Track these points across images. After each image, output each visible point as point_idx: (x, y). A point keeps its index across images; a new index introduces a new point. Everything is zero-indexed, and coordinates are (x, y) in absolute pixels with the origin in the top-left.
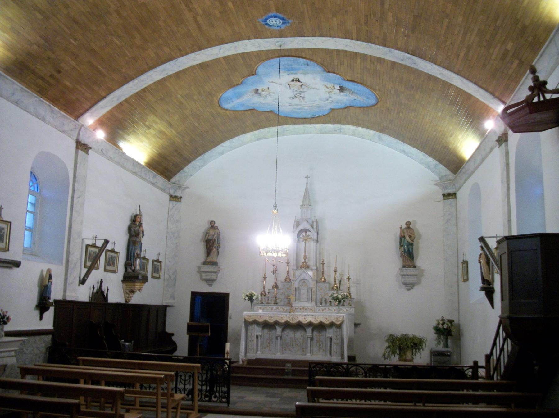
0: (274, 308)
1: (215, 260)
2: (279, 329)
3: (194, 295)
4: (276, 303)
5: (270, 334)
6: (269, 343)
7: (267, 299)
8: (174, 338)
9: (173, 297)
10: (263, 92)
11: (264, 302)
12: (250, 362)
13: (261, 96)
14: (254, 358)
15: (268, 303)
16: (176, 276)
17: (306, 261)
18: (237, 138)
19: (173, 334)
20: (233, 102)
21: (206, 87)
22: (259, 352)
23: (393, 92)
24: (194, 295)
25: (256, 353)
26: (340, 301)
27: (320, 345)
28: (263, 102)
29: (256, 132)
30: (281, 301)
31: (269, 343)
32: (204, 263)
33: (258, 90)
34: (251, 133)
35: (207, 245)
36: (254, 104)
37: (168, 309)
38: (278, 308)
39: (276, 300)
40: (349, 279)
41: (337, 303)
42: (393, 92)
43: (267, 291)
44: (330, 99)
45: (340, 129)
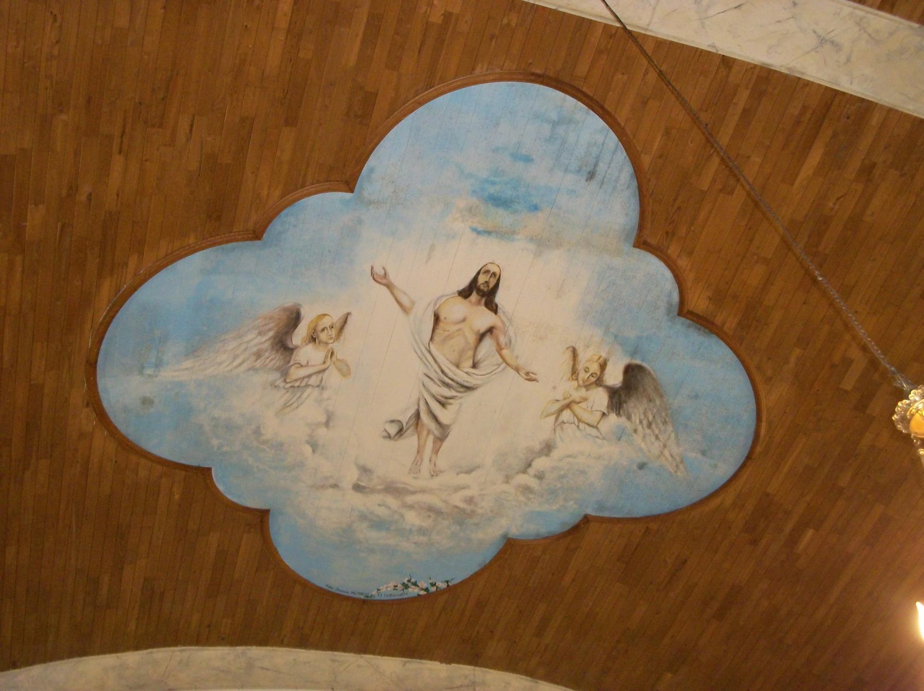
10: (310, 347)
13: (284, 373)
18: (37, 670)
20: (159, 365)
21: (118, 163)
23: (848, 384)
28: (272, 428)
29: (132, 658)
33: (294, 318)
34: (109, 660)
36: (230, 427)
42: (848, 384)
44: (541, 463)
45: (474, 684)
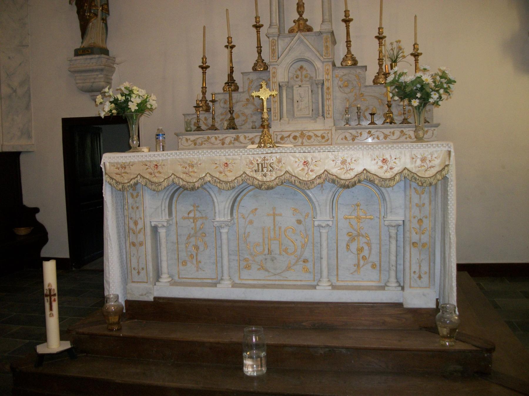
0: (227, 141)
1: (100, 44)
2: (222, 203)
3: (66, 122)
4: (232, 126)
5: (195, 219)
6: (197, 248)
7: (210, 121)
8: (39, 217)
9: (27, 133)
11: (203, 127)
12: (136, 309)
14: (151, 299)
15: (213, 128)
16: (29, 89)
17: (305, 16)
19: (37, 210)
22: (165, 278)
24: (66, 122)
25: (158, 277)
26: (425, 100)
27: (361, 250)
30: (245, 122)
31: (197, 248)
32: (78, 53)
35: (78, 12)
37: (22, 157)
38: (237, 139)
39: (232, 119)
40: (416, 55)
41: (415, 103)
43: (209, 97)
